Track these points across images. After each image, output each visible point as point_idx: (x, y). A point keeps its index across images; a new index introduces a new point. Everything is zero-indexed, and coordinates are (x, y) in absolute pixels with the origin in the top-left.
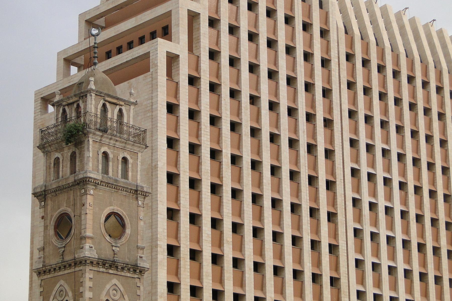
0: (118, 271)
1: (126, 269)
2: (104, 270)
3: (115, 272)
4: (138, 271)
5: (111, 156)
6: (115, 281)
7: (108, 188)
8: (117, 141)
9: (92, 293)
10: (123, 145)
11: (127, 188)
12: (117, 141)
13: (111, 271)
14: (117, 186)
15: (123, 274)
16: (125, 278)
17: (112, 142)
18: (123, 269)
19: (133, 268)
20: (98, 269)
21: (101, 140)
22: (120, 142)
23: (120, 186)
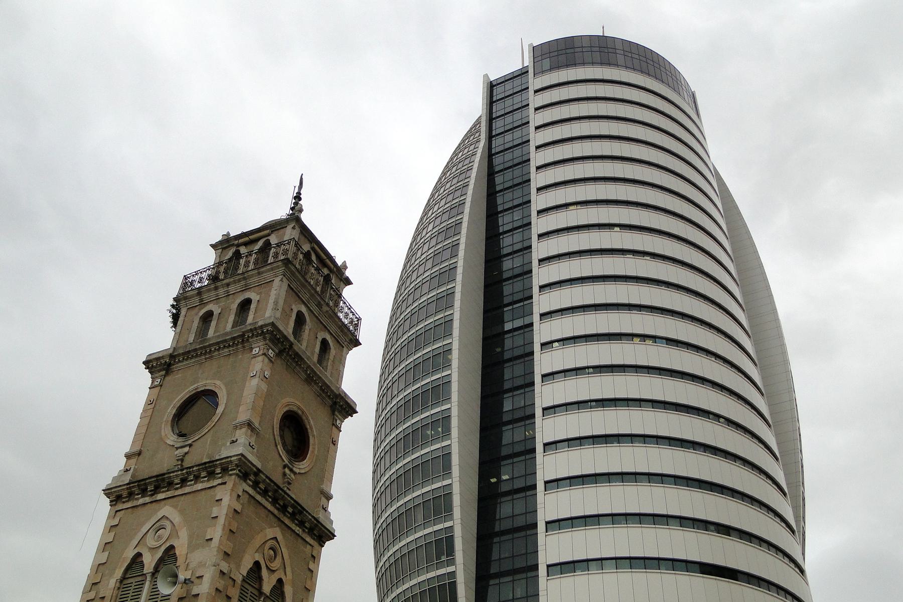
0: (177, 489)
1: (191, 477)
2: (147, 499)
3: (169, 494)
4: (218, 470)
5: (216, 313)
6: (167, 510)
7: (193, 360)
8: (228, 285)
9: (107, 553)
10: (243, 283)
11: (225, 341)
12: (228, 285)
13: (160, 496)
14: (205, 347)
15: (187, 490)
16: (192, 495)
17: (221, 291)
18: (184, 481)
19: (204, 469)
20: (135, 503)
21: (201, 300)
22: (234, 282)
23: (210, 345)
